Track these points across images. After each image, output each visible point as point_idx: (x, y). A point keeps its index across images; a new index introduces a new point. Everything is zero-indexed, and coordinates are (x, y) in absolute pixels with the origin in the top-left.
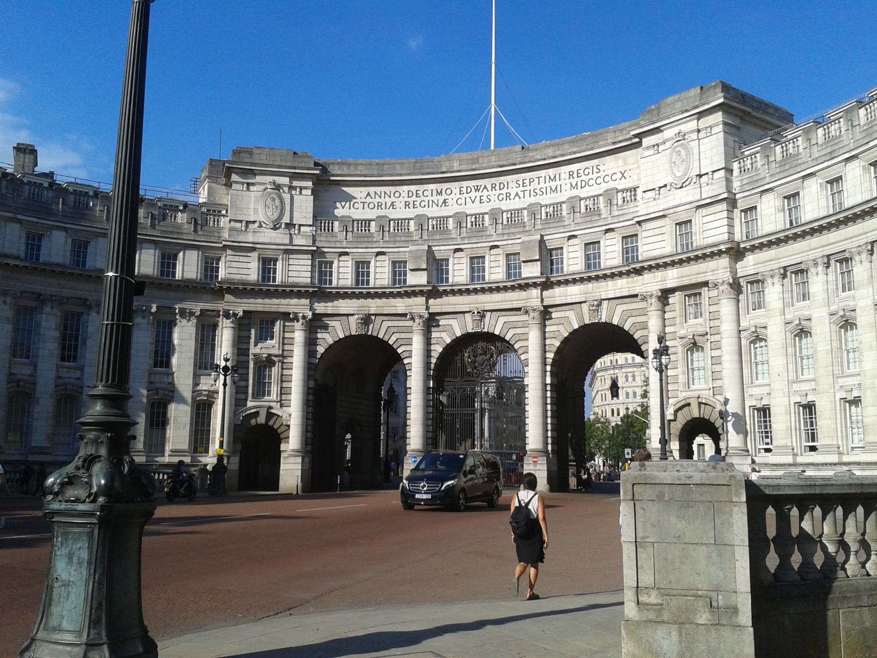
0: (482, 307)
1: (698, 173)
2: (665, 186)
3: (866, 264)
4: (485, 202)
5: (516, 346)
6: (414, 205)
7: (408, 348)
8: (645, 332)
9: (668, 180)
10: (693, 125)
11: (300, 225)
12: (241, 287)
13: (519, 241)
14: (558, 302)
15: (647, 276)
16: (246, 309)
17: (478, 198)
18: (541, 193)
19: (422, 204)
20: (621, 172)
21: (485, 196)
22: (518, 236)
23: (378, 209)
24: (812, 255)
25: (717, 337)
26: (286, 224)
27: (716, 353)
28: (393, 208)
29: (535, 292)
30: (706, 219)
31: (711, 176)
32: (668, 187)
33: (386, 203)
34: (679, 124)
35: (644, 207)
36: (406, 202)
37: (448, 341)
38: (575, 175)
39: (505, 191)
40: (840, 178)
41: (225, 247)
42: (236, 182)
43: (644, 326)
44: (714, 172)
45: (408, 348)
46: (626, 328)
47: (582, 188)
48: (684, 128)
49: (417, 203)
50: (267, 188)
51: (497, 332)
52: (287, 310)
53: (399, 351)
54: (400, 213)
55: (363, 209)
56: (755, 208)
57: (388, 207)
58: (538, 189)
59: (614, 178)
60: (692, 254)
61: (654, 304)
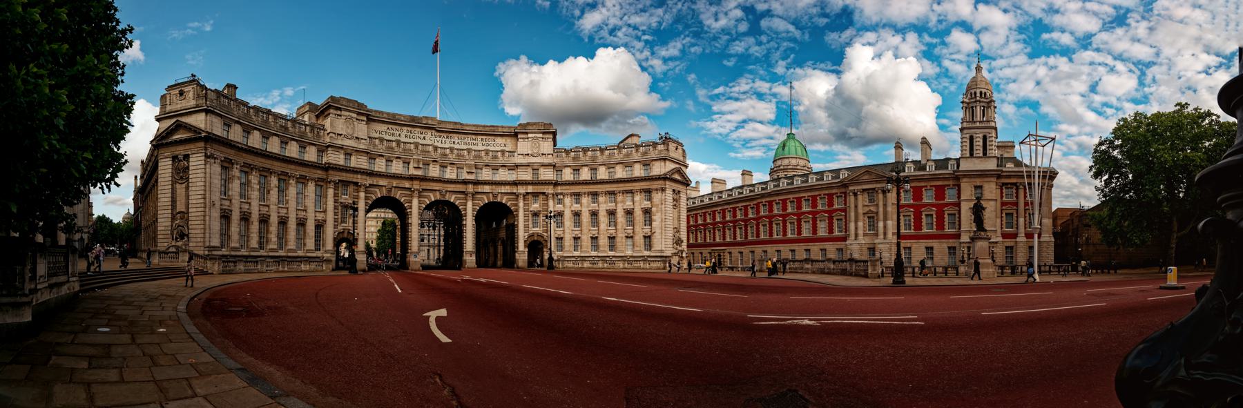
3: (604, 197)
7: (410, 204)
8: (516, 208)
9: (530, 152)
14: (480, 191)
24: (583, 191)
26: (356, 138)
29: (470, 186)
35: (518, 160)
37: (428, 203)
40: (596, 169)
41: (329, 146)
45: (410, 204)
46: (508, 205)
51: (452, 201)
53: (406, 205)
54: (403, 139)
56: (562, 170)
61: (521, 198)
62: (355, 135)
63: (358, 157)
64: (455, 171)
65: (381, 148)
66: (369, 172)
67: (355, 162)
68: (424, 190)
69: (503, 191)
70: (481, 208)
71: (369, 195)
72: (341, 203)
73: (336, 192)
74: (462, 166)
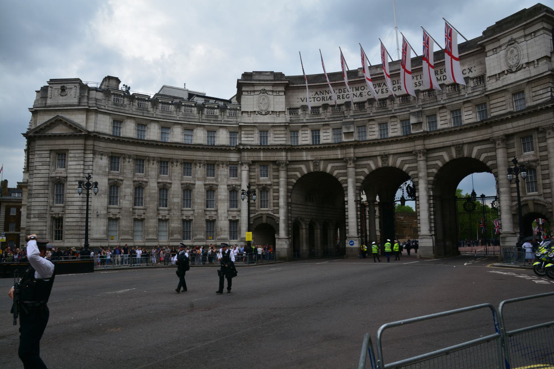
0: (387, 152)
1: (527, 62)
2: (503, 72)
4: (385, 92)
5: (411, 174)
6: (343, 97)
7: (344, 178)
8: (494, 162)
9: (505, 68)
10: (521, 33)
11: (279, 112)
12: (249, 147)
13: (408, 112)
15: (495, 128)
16: (253, 159)
17: (380, 91)
18: (419, 85)
19: (348, 96)
20: (468, 69)
21: (385, 89)
22: (407, 109)
23: (322, 100)
25: (545, 163)
26: (272, 112)
27: (546, 172)
28: (331, 100)
30: (534, 89)
31: (536, 63)
32: (506, 72)
33: (327, 97)
34: (511, 34)
36: (338, 96)
38: (439, 73)
39: (396, 85)
42: (245, 91)
43: (494, 158)
44: (538, 60)
45: (344, 178)
47: (444, 80)
48: (515, 36)
49: (345, 96)
50: (261, 93)
52: (275, 159)
55: (314, 101)
57: (328, 99)
58: (418, 82)
59: (464, 72)
60: (526, 111)
62: (271, 109)
63: (275, 132)
64: (399, 126)
65: (304, 118)
66: (287, 147)
67: (272, 140)
68: (359, 158)
69: (470, 140)
70: (441, 170)
71: (293, 173)
72: (258, 185)
73: (252, 174)
74: (406, 117)
